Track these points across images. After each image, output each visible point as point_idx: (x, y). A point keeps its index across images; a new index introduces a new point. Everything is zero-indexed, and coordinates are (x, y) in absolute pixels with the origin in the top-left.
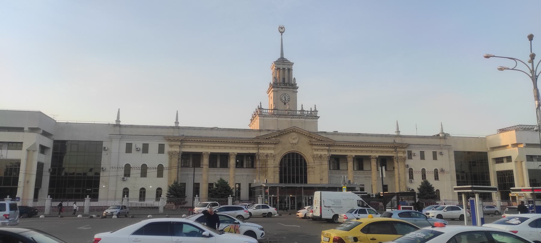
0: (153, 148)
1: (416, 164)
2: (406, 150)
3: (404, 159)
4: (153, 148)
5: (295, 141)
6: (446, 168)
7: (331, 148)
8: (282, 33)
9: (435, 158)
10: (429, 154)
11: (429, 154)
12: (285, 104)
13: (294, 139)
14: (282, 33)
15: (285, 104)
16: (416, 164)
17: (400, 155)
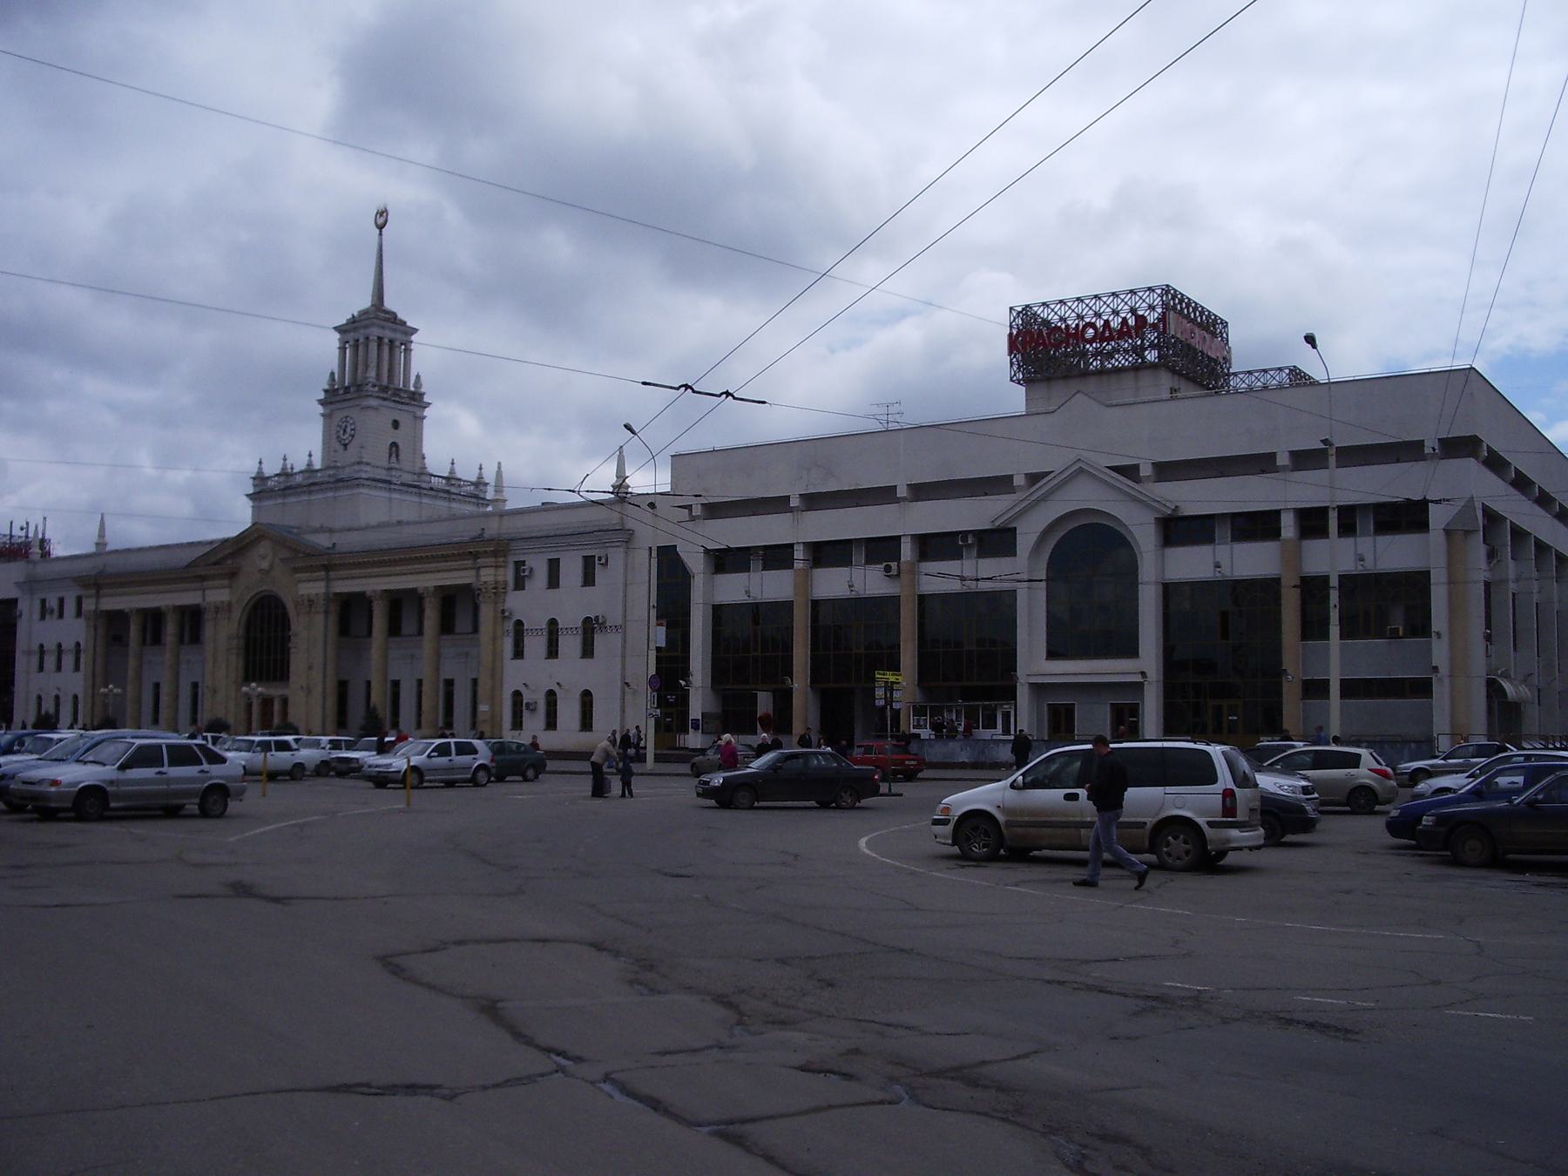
0: (70, 607)
1: (532, 605)
2: (512, 559)
3: (499, 591)
4: (70, 607)
5: (265, 565)
6: (614, 618)
7: (332, 574)
8: (381, 228)
9: (589, 580)
10: (571, 569)
11: (571, 569)
12: (345, 446)
13: (264, 558)
14: (381, 228)
15: (345, 446)
16: (532, 605)
17: (488, 575)
